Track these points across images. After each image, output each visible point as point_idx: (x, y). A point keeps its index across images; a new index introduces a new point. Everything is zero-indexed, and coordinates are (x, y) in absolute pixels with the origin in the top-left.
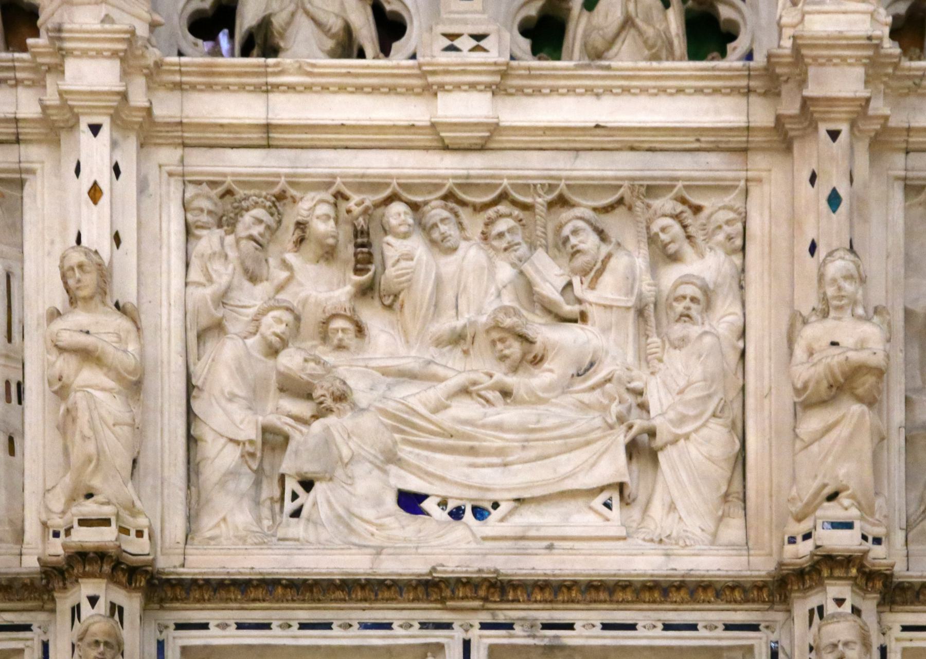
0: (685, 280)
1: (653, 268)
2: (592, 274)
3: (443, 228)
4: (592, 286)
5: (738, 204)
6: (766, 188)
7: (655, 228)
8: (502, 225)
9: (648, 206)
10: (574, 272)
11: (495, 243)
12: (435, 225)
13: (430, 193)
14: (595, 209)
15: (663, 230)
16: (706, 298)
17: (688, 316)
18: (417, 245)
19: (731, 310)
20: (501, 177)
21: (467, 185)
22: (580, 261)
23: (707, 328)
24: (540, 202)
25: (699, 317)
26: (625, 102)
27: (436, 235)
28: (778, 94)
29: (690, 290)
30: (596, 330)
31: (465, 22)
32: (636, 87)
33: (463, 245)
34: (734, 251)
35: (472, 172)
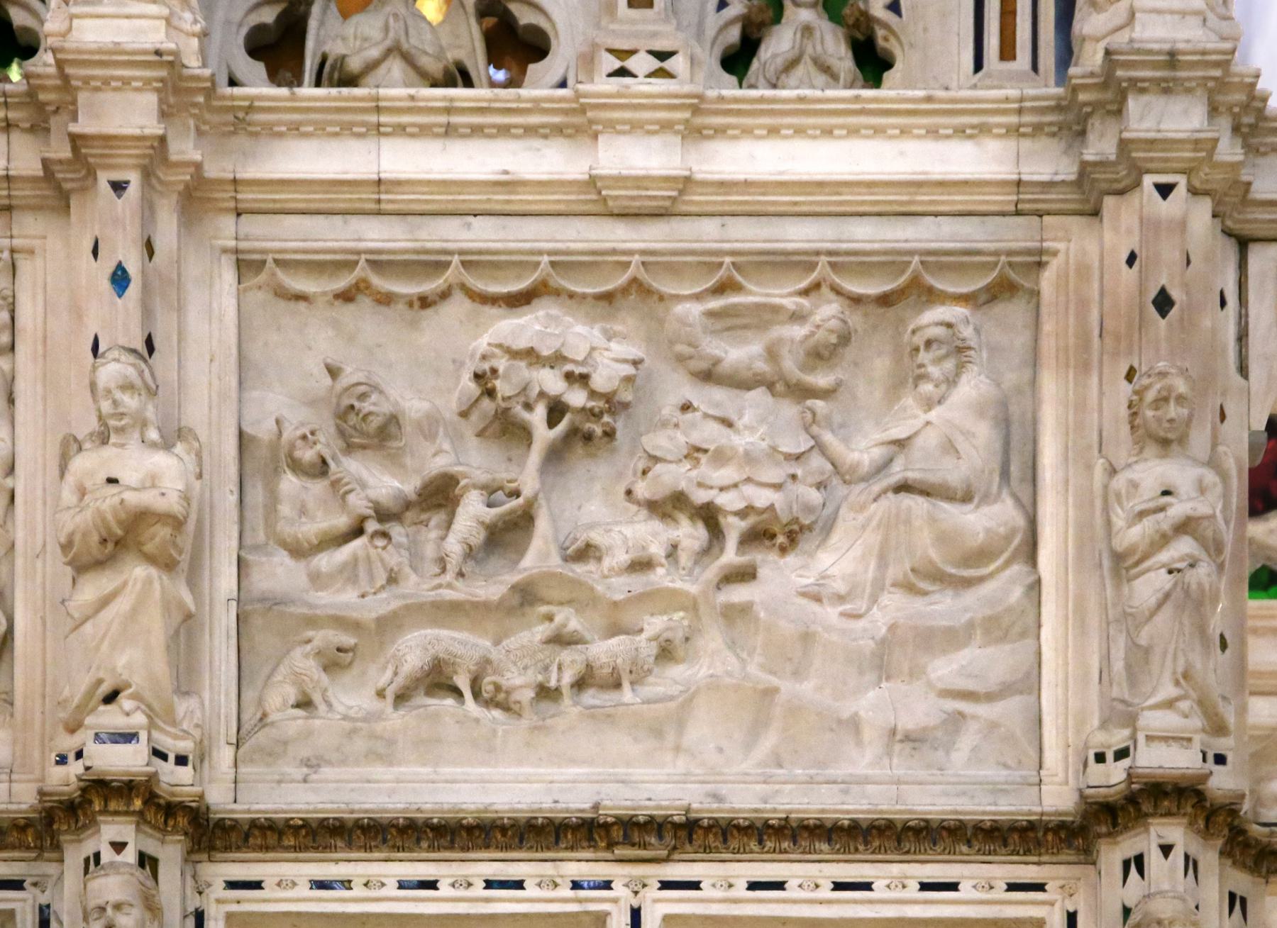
6: (39, 262)
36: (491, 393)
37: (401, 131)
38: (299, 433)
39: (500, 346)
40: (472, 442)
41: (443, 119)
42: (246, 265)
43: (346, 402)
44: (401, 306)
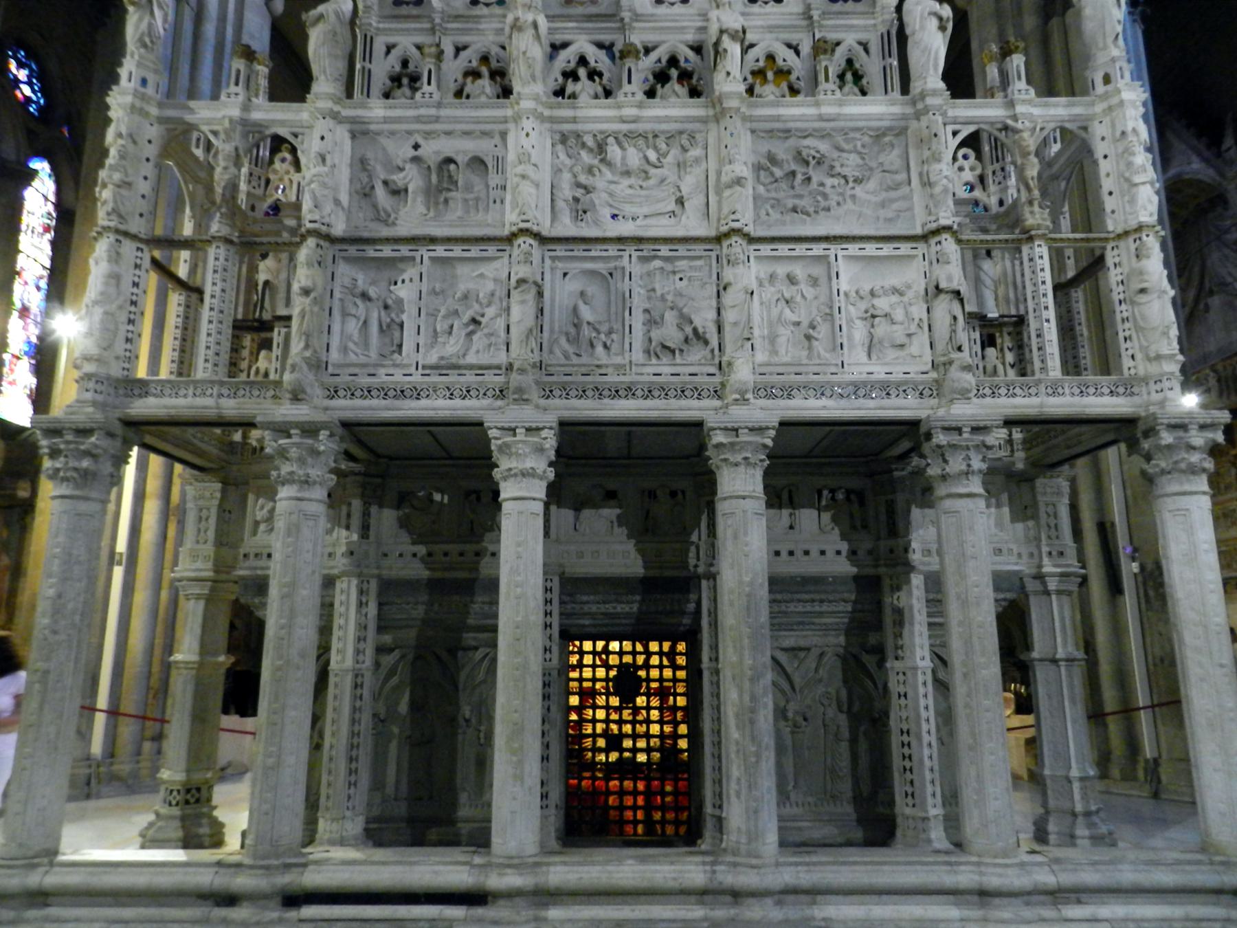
18: (616, 148)
21: (631, 132)
42: (753, 132)
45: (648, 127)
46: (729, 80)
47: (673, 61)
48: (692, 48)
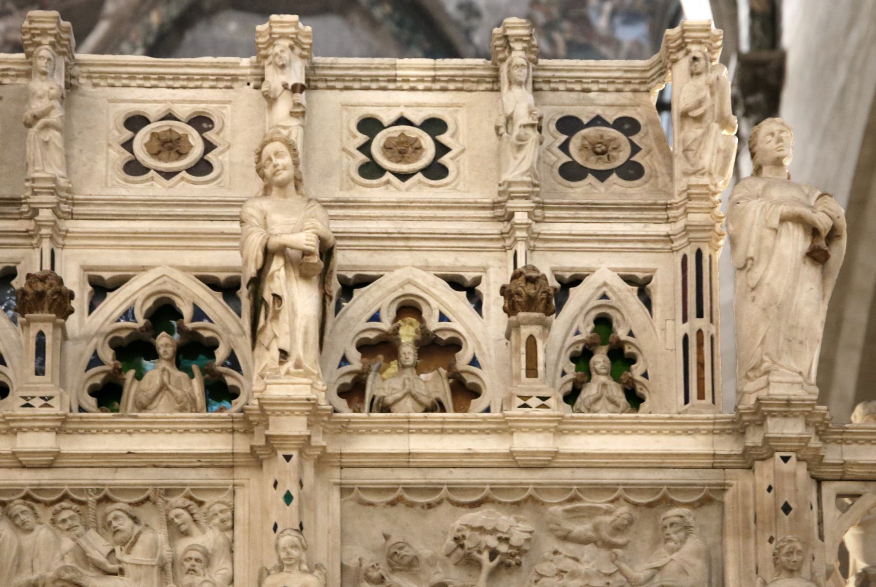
0: (191, 548)
1: (171, 540)
2: (128, 544)
3: (23, 517)
4: (128, 552)
5: (228, 500)
6: (247, 491)
7: (172, 515)
8: (65, 515)
9: (167, 502)
10: (117, 543)
11: (60, 526)
12: (17, 515)
13: (13, 495)
14: (130, 504)
15: (177, 516)
16: (207, 559)
17: (193, 570)
19: (224, 566)
20: (63, 485)
21: (39, 490)
22: (119, 536)
23: (207, 578)
24: (91, 499)
25: (201, 571)
26: (149, 437)
27: (18, 522)
28: (253, 433)
29: (194, 554)
30: (130, 579)
31: (38, 389)
32: (156, 429)
33: (38, 527)
34: (227, 530)
35: (42, 482)
36: (462, 546)
37: (420, 431)
38: (371, 564)
39: (466, 525)
40: (452, 567)
41: (440, 426)
42: (345, 490)
43: (393, 550)
44: (418, 508)
45: (87, 477)
46: (288, 363)
47: (164, 312)
48: (213, 284)
